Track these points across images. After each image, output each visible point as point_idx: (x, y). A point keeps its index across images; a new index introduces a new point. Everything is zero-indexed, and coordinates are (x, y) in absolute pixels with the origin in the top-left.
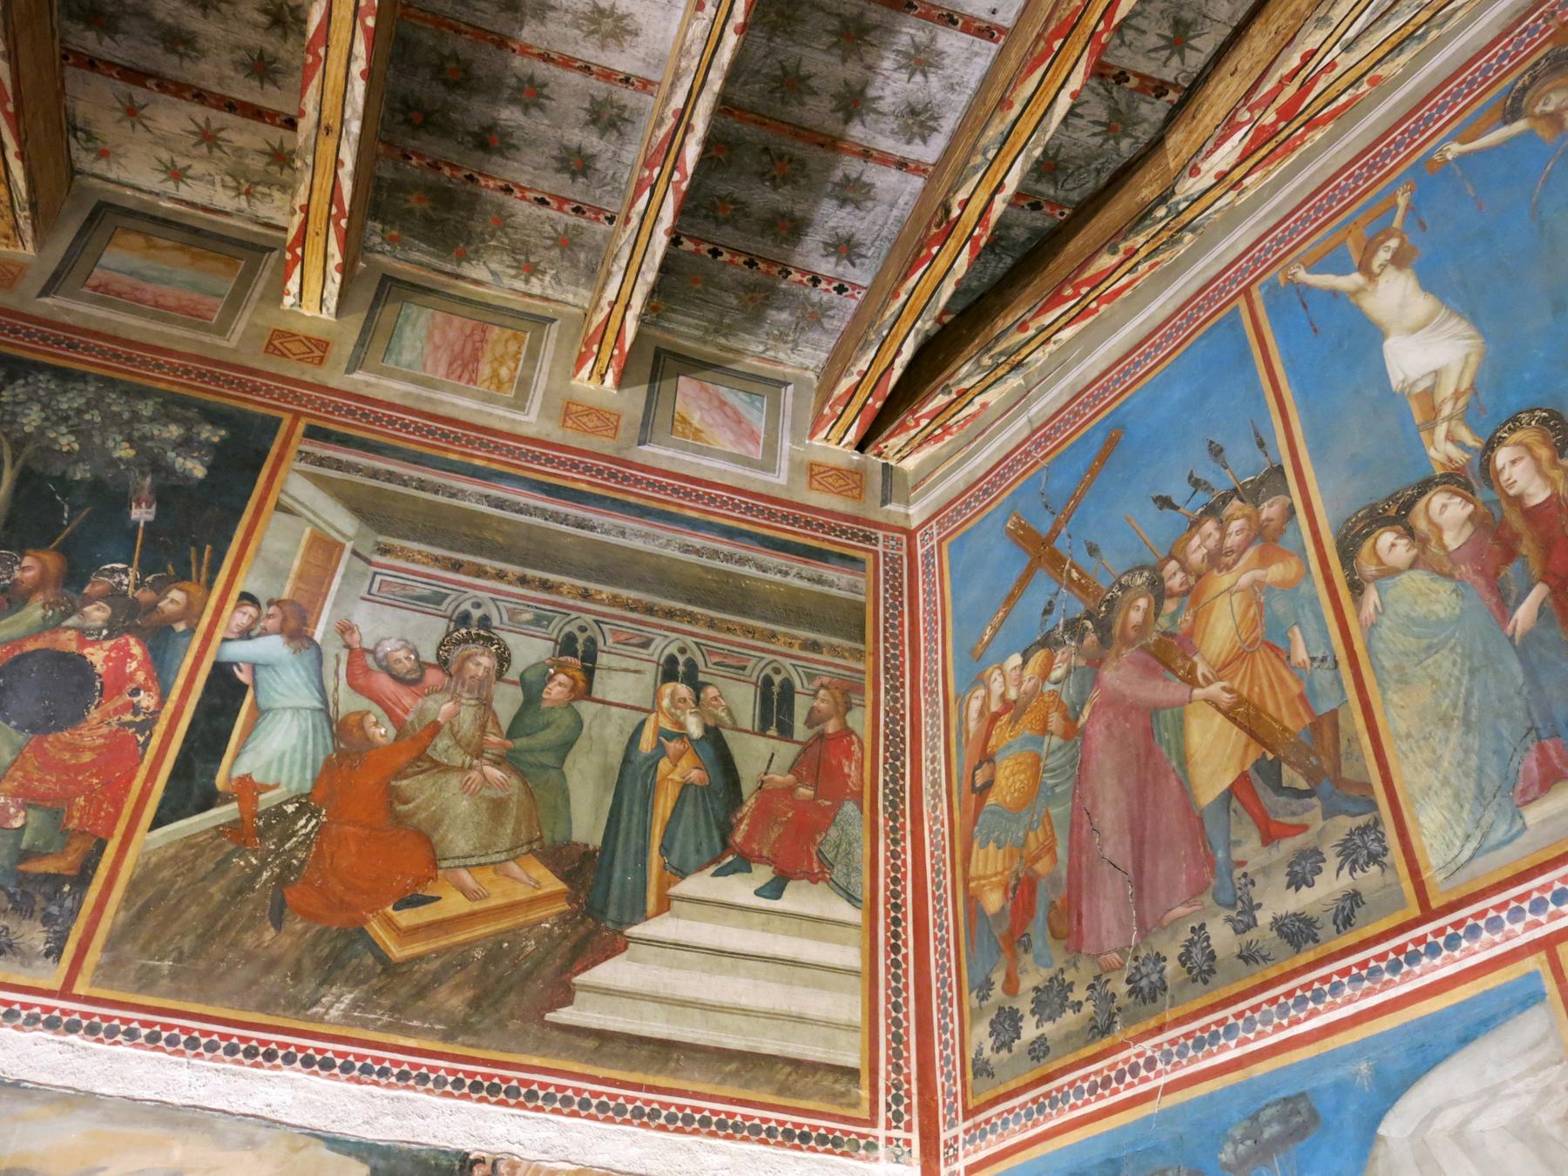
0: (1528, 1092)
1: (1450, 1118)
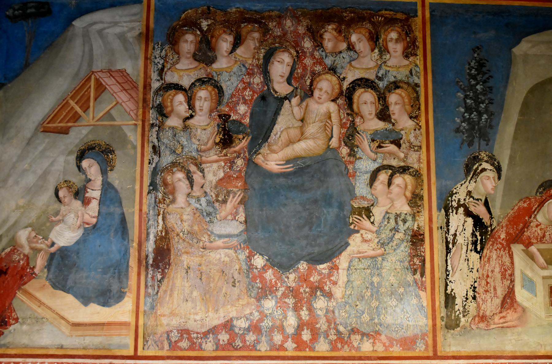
0: (127, 27)
1: (99, 27)
